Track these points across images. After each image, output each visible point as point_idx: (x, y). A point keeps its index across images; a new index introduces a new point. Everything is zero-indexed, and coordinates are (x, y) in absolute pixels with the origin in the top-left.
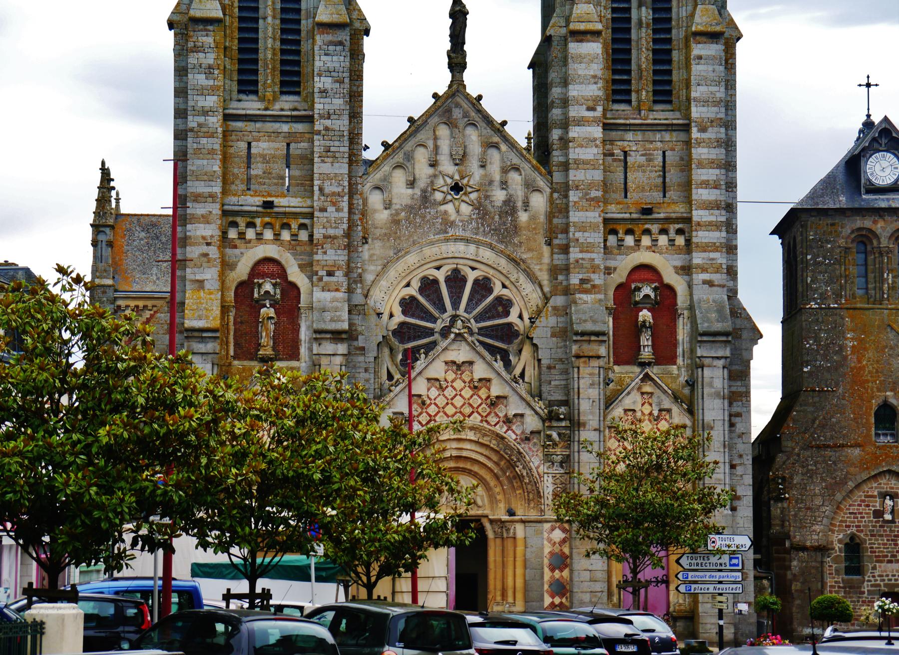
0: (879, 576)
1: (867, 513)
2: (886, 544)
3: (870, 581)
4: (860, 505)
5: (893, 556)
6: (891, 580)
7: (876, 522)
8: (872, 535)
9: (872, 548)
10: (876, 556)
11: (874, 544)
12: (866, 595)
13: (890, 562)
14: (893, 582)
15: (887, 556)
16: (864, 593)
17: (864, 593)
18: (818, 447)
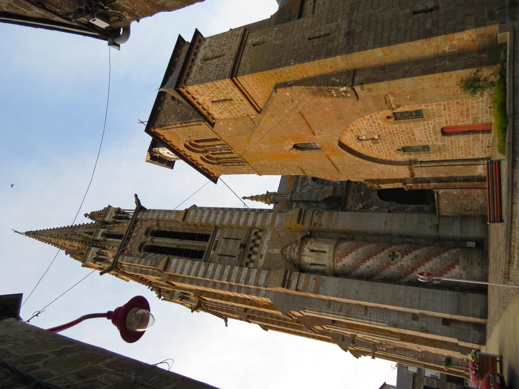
0: (427, 138)
1: (377, 146)
2: (399, 138)
3: (433, 142)
4: (372, 150)
5: (408, 133)
6: (430, 134)
7: (382, 142)
8: (393, 143)
9: (404, 143)
10: (410, 140)
11: (401, 143)
12: (446, 144)
13: (413, 135)
14: (431, 132)
15: (409, 137)
16: (444, 145)
17: (444, 145)
18: (338, 170)
